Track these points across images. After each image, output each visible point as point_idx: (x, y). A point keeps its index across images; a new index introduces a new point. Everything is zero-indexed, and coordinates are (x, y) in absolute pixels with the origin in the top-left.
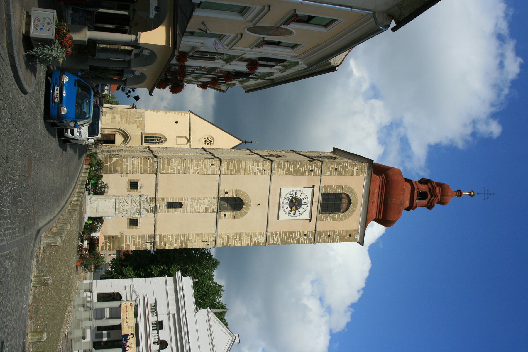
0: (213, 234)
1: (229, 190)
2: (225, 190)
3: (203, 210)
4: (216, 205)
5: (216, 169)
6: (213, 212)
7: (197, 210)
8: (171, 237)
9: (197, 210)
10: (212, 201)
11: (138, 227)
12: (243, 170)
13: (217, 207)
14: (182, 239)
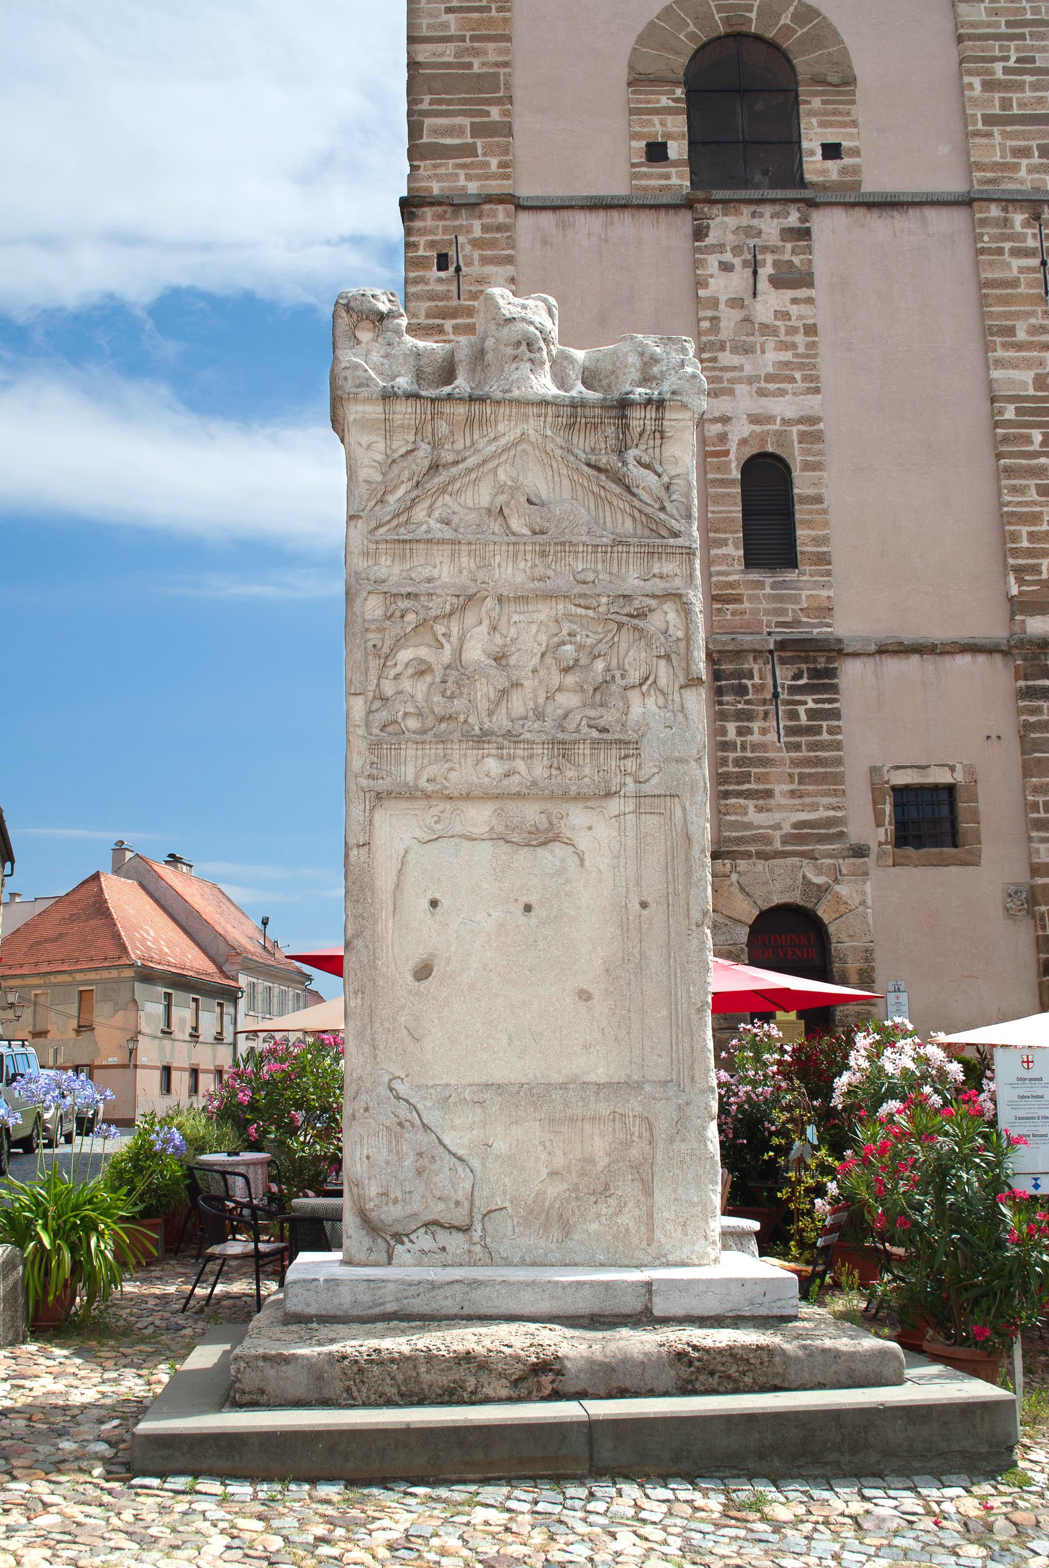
0: (983, 222)
1: (635, 136)
2: (633, 165)
3: (794, 301)
4: (754, 215)
5: (477, 233)
6: (804, 234)
7: (801, 350)
8: (1025, 530)
9: (801, 350)
10: (720, 248)
11: (959, 777)
12: (476, 53)
13: (767, 210)
14: (1035, 447)
